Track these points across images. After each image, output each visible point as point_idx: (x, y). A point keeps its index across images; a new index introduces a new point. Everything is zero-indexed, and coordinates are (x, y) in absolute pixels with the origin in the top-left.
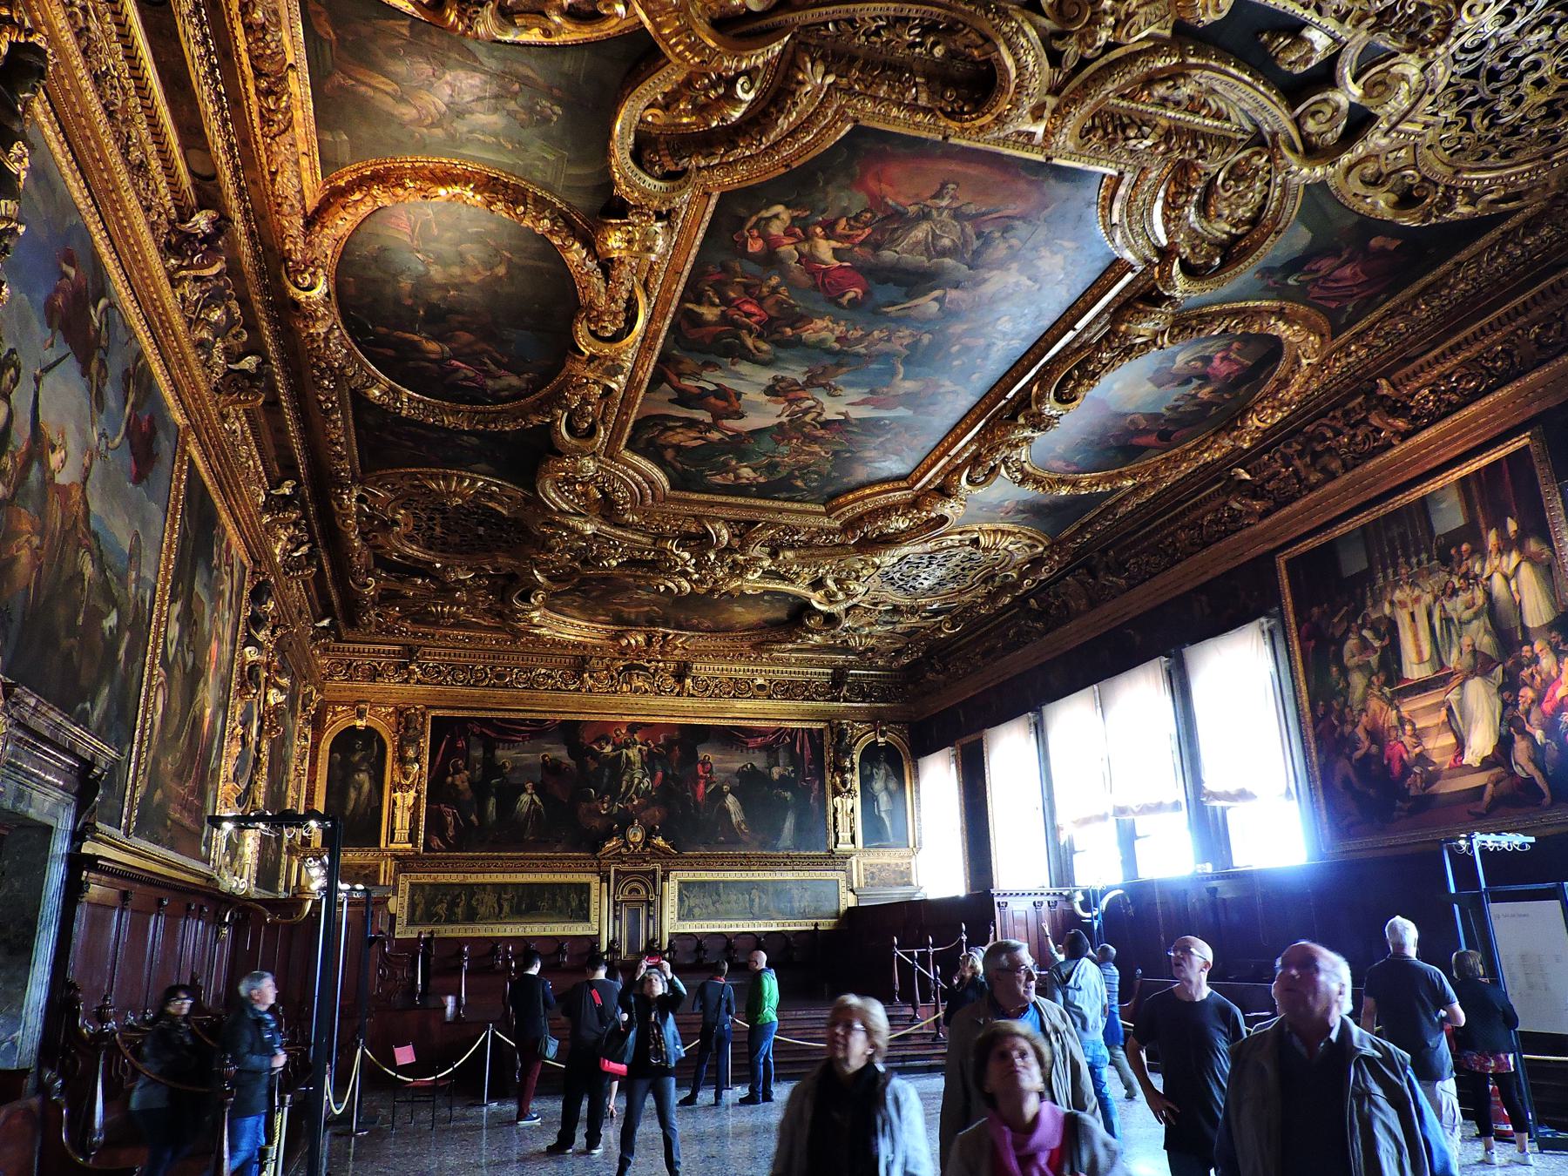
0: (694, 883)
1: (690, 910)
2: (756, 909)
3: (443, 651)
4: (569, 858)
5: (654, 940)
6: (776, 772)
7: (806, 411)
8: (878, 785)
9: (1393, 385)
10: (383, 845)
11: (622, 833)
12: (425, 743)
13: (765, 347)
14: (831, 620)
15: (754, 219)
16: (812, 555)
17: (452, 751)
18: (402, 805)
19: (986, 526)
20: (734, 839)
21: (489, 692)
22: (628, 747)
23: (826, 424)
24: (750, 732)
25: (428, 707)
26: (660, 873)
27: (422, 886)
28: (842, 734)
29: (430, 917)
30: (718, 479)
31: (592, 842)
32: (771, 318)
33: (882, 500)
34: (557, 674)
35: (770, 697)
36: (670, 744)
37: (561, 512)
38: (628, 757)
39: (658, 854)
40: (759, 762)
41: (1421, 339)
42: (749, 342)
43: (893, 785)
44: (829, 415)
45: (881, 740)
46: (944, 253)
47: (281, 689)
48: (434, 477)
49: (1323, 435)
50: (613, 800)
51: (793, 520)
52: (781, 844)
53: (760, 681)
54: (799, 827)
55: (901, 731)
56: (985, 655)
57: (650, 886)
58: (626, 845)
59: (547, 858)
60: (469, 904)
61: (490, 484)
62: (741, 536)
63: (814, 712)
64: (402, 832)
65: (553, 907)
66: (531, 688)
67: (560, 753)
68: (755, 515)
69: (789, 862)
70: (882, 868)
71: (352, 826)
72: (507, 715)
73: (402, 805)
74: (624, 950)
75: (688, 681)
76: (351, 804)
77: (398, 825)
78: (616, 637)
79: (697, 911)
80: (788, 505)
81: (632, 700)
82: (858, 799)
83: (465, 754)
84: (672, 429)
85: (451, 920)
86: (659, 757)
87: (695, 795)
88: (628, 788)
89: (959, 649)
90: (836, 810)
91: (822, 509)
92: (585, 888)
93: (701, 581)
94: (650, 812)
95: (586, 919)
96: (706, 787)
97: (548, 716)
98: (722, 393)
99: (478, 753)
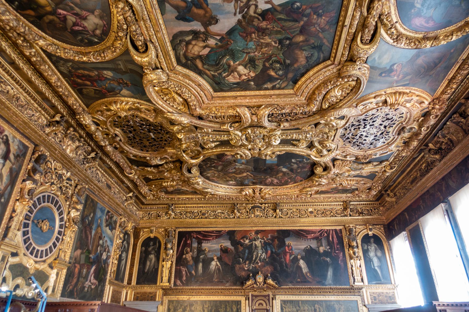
3: (182, 206)
4: (231, 289)
6: (322, 249)
8: (372, 254)
10: (158, 284)
12: (175, 242)
14: (326, 169)
17: (186, 245)
18: (167, 267)
19: (389, 91)
20: (305, 281)
22: (255, 240)
24: (308, 232)
25: (176, 228)
26: (271, 296)
28: (350, 231)
31: (241, 282)
35: (315, 216)
36: (273, 239)
37: (169, 112)
38: (255, 245)
39: (270, 287)
43: (379, 254)
47: (77, 210)
50: (250, 263)
51: (281, 101)
52: (327, 283)
53: (310, 210)
54: (335, 274)
55: (380, 229)
56: (412, 182)
57: (267, 302)
58: (256, 283)
63: (336, 221)
64: (165, 278)
66: (216, 218)
67: (227, 244)
69: (331, 291)
70: (379, 295)
71: (148, 276)
72: (207, 229)
73: (167, 267)
75: (278, 211)
76: (147, 267)
77: (164, 276)
78: (242, 190)
82: (362, 262)
83: (190, 246)
86: (269, 244)
87: (285, 259)
88: (256, 258)
89: (399, 183)
90: (352, 266)
92: (238, 303)
93: (253, 149)
94: (266, 268)
96: (290, 256)
99: (195, 245)
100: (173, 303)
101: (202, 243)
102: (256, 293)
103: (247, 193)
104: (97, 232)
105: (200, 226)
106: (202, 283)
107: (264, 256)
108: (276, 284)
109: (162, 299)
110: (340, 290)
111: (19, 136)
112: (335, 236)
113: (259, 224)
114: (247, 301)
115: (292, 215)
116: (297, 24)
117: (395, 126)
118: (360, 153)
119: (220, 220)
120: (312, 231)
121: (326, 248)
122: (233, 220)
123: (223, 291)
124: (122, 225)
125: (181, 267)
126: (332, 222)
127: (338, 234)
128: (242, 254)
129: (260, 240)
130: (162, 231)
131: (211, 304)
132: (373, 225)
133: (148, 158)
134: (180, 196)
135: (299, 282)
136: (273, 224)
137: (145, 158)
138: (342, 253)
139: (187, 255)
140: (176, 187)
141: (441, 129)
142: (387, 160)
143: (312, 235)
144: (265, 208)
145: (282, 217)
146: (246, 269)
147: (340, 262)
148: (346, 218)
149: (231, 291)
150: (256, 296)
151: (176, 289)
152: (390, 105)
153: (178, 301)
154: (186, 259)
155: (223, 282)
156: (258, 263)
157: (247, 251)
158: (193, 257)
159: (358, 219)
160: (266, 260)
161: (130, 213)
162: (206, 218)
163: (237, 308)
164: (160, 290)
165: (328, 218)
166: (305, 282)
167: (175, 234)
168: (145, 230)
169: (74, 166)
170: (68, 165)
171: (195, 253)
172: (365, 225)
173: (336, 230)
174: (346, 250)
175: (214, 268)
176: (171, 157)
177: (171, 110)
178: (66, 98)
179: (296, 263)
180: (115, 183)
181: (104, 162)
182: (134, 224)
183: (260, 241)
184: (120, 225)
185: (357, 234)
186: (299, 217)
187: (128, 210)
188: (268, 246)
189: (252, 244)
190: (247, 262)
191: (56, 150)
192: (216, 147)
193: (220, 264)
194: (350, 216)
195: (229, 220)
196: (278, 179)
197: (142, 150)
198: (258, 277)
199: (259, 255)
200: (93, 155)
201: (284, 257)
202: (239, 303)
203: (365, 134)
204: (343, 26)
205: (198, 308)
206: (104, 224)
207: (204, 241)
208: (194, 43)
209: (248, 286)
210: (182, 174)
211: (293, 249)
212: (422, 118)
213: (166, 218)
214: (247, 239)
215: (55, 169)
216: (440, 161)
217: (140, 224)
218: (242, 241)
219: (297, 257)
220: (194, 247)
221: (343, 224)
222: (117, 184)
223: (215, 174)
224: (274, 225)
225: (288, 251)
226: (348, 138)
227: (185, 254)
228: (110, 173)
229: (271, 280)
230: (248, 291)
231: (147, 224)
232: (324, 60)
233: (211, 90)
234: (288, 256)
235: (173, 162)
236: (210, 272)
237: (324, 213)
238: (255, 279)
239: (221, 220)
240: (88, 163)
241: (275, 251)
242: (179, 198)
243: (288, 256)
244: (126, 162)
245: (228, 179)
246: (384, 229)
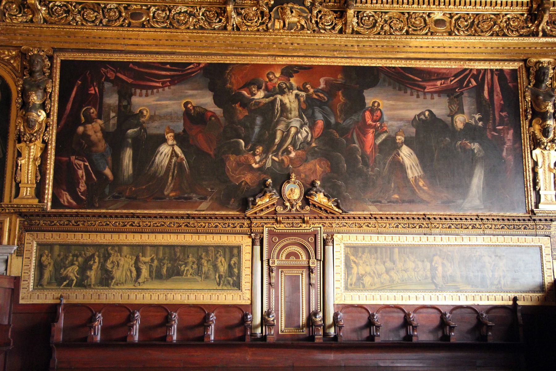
0: (364, 248)
1: (360, 278)
2: (439, 280)
5: (315, 314)
6: (460, 121)
10: (6, 200)
11: (279, 186)
17: (84, 99)
22: (282, 92)
27: (50, 246)
28: (539, 74)
29: (59, 280)
35: (450, 34)
36: (331, 90)
38: (283, 105)
40: (440, 108)
50: (266, 152)
52: (467, 204)
53: (438, 15)
58: (282, 201)
59: (189, 216)
60: (103, 268)
63: (506, 49)
65: (199, 272)
67: (205, 100)
72: (145, 59)
74: (282, 325)
75: (351, 12)
79: (367, 280)
85: (82, 283)
86: (321, 104)
87: (362, 143)
88: (284, 140)
90: (536, 164)
92: (234, 252)
94: (309, 166)
95: (237, 285)
96: (376, 137)
97: (192, 59)
99: (112, 100)
100: (51, 251)
101: (131, 95)
102: (280, 228)
106: (133, 200)
107: (305, 134)
108: (338, 207)
109: (20, 239)
110: (501, 222)
113: (295, 50)
114: (257, 248)
119: (183, 34)
120: (438, 74)
121: (472, 117)
123: (192, 221)
125: (73, 158)
126: (496, 50)
128: (246, 127)
129: (296, 92)
130: (12, 57)
131: (157, 254)
135: (396, 202)
136: (335, 50)
138: (511, 132)
139: (89, 126)
143: (439, 83)
145: (358, 33)
146: (255, 166)
147: (504, 154)
148: (532, 40)
149: (214, 222)
150: (282, 236)
151: (61, 215)
153: (67, 247)
154: (85, 135)
155: (190, 198)
156: (290, 152)
157: (259, 120)
158: (106, 134)
160: (309, 144)
162: (143, 26)
163: (230, 266)
164: (14, 217)
166: (411, 202)
167: (51, 68)
171: (113, 121)
173: (501, 71)
174: (525, 124)
175: (166, 162)
179: (390, 154)
183: (297, 96)
186: (407, 33)
188: (317, 110)
189: (273, 102)
190: (259, 149)
193: (184, 152)
194: (545, 35)
198: (287, 188)
199: (293, 130)
201: (358, 136)
202: (235, 251)
205: (122, 263)
207: (138, 91)
209: (262, 210)
211: (385, 118)
213: (21, 18)
214: (259, 88)
218: (245, 93)
219: (394, 139)
220: (109, 106)
221: (521, 58)
225: (370, 122)
227: (84, 125)
229: (321, 195)
230: (258, 221)
234: (370, 136)
236: (156, 172)
237: (474, 26)
238: (280, 193)
239: (187, 35)
241: (337, 124)
243: (370, 136)
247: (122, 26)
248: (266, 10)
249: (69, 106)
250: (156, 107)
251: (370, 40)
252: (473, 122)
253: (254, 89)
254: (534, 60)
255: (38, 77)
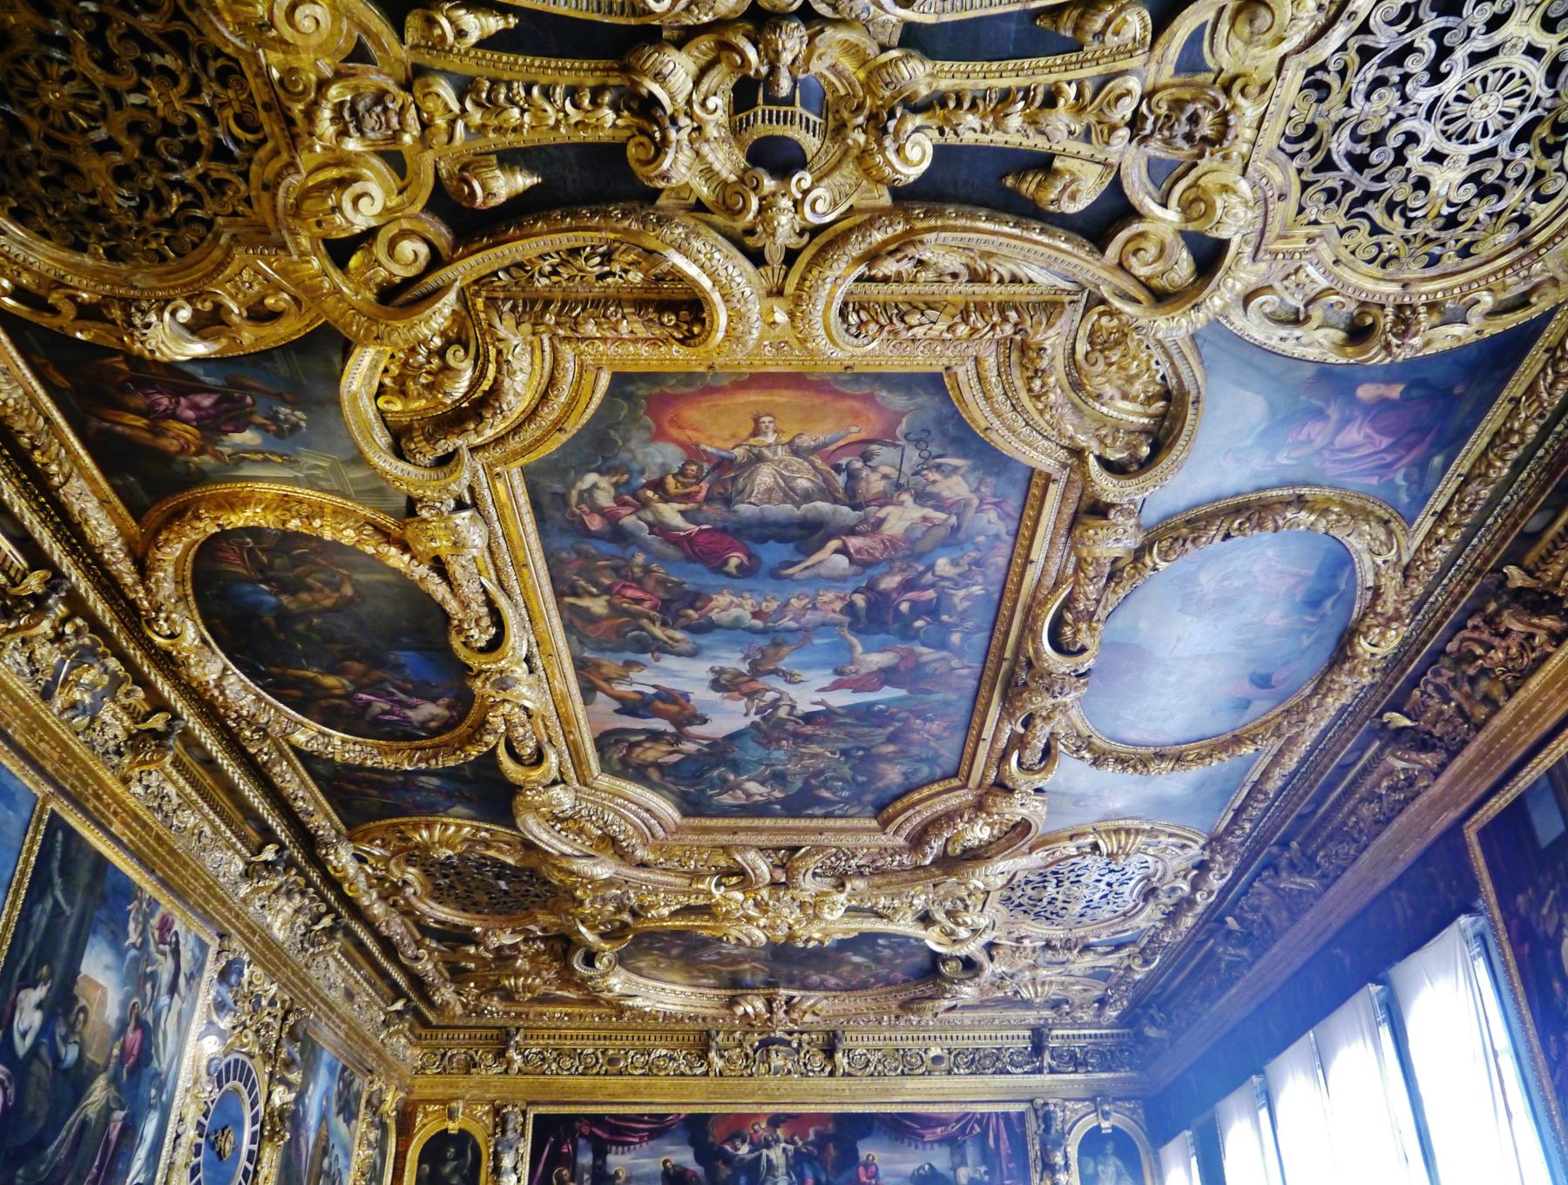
3: (546, 1033)
7: (775, 704)
9: (1530, 573)
12: (526, 1148)
13: (678, 635)
14: (970, 966)
15: (574, 493)
16: (890, 883)
17: (557, 1159)
21: (600, 1080)
22: (768, 1146)
23: (809, 718)
25: (530, 1104)
28: (1047, 1119)
30: (727, 799)
32: (664, 601)
33: (939, 807)
34: (680, 1055)
35: (949, 1072)
37: (563, 855)
38: (769, 1161)
40: (940, 1159)
41: (1530, 505)
42: (658, 631)
44: (804, 707)
45: (1105, 1124)
46: (808, 497)
48: (416, 827)
49: (1471, 652)
51: (847, 841)
53: (935, 1051)
55: (1133, 1111)
61: (478, 829)
62: (783, 866)
67: (684, 1157)
68: (794, 840)
75: (839, 1056)
78: (732, 1003)
80: (830, 823)
81: (773, 1084)
84: (639, 744)
91: (874, 824)
98: (666, 696)
99: (586, 1159)
101: (606, 1153)
103: (750, 1009)
104: (318, 1138)
105: (601, 1099)
111: (196, 925)
112: (1004, 1135)
115: (880, 1068)
116: (880, 731)
117: (1132, 883)
118: (1057, 934)
121: (976, 1171)
122: (704, 1081)
124: (375, 1101)
127: (1013, 1124)
132: (1115, 1099)
133: (478, 930)
134: (544, 1009)
137: (470, 928)
140: (542, 989)
141: (1245, 893)
142: (1133, 942)
143: (939, 1130)
144: (800, 1044)
145: (850, 1075)
148: (1038, 1077)
152: (1108, 855)
159: (1072, 1082)
161: (392, 1059)
162: (621, 1074)
165: (986, 1078)
167: (524, 1124)
168: (431, 1108)
169: (285, 965)
170: (274, 965)
172: (1093, 1100)
173: (1006, 1115)
176: (544, 930)
177: (568, 850)
178: (305, 819)
180: (365, 979)
181: (349, 932)
182: (402, 1095)
183: (784, 1150)
184: (368, 1102)
185: (1067, 1128)
186: (903, 1073)
187: (388, 1052)
189: (759, 1158)
191: (254, 933)
192: (673, 914)
194: (1052, 1071)
195: (692, 1081)
196: (840, 977)
197: (465, 910)
200: (327, 921)
203: (1061, 897)
204: (979, 738)
206: (334, 1109)
208: (647, 745)
210: (568, 968)
212: (1195, 872)
214: (743, 1142)
215: (250, 983)
216: (1250, 966)
217: (416, 1089)
218: (728, 1148)
220: (583, 1167)
222: (369, 983)
223: (659, 963)
224: (827, 1099)
226: (1020, 905)
228: (358, 956)
231: (436, 1090)
232: (945, 777)
233: (676, 815)
235: (543, 939)
237: (977, 1063)
239: (667, 1082)
240: (313, 945)
242: (542, 1014)
244: (409, 932)
245: (696, 973)
246: (1146, 1112)
247: (598, 1074)
248: (749, 1051)
249: (541, 1168)
250: (630, 1168)
251: (861, 1084)
252: (977, 1176)
253: (738, 1143)
254: (1040, 1101)
255: (510, 1135)
